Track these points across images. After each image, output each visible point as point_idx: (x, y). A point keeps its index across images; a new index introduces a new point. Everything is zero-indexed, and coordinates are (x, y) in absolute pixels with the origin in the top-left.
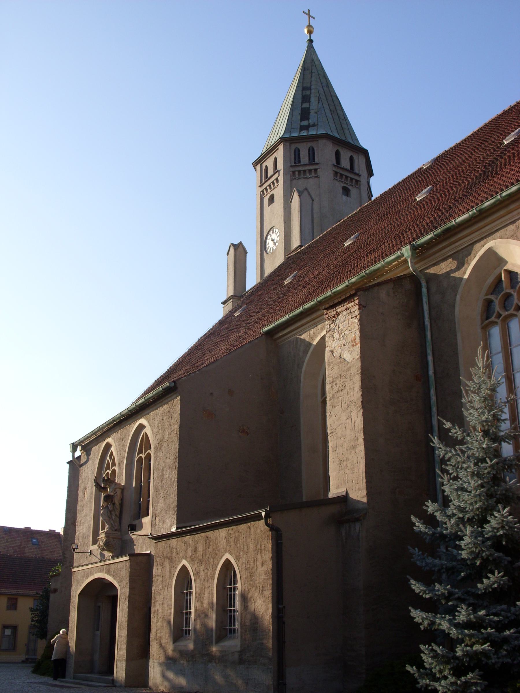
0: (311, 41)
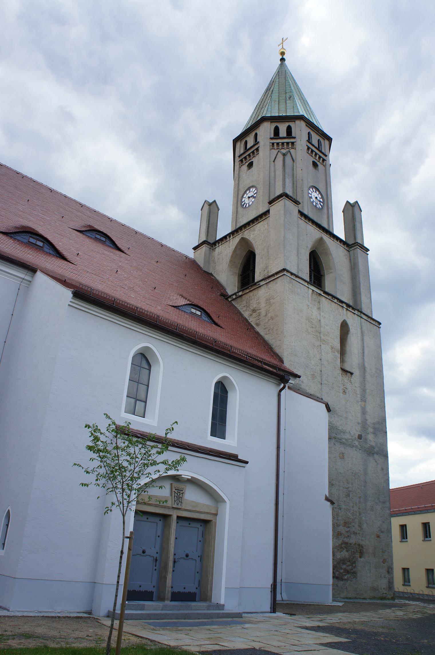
0: (283, 60)
